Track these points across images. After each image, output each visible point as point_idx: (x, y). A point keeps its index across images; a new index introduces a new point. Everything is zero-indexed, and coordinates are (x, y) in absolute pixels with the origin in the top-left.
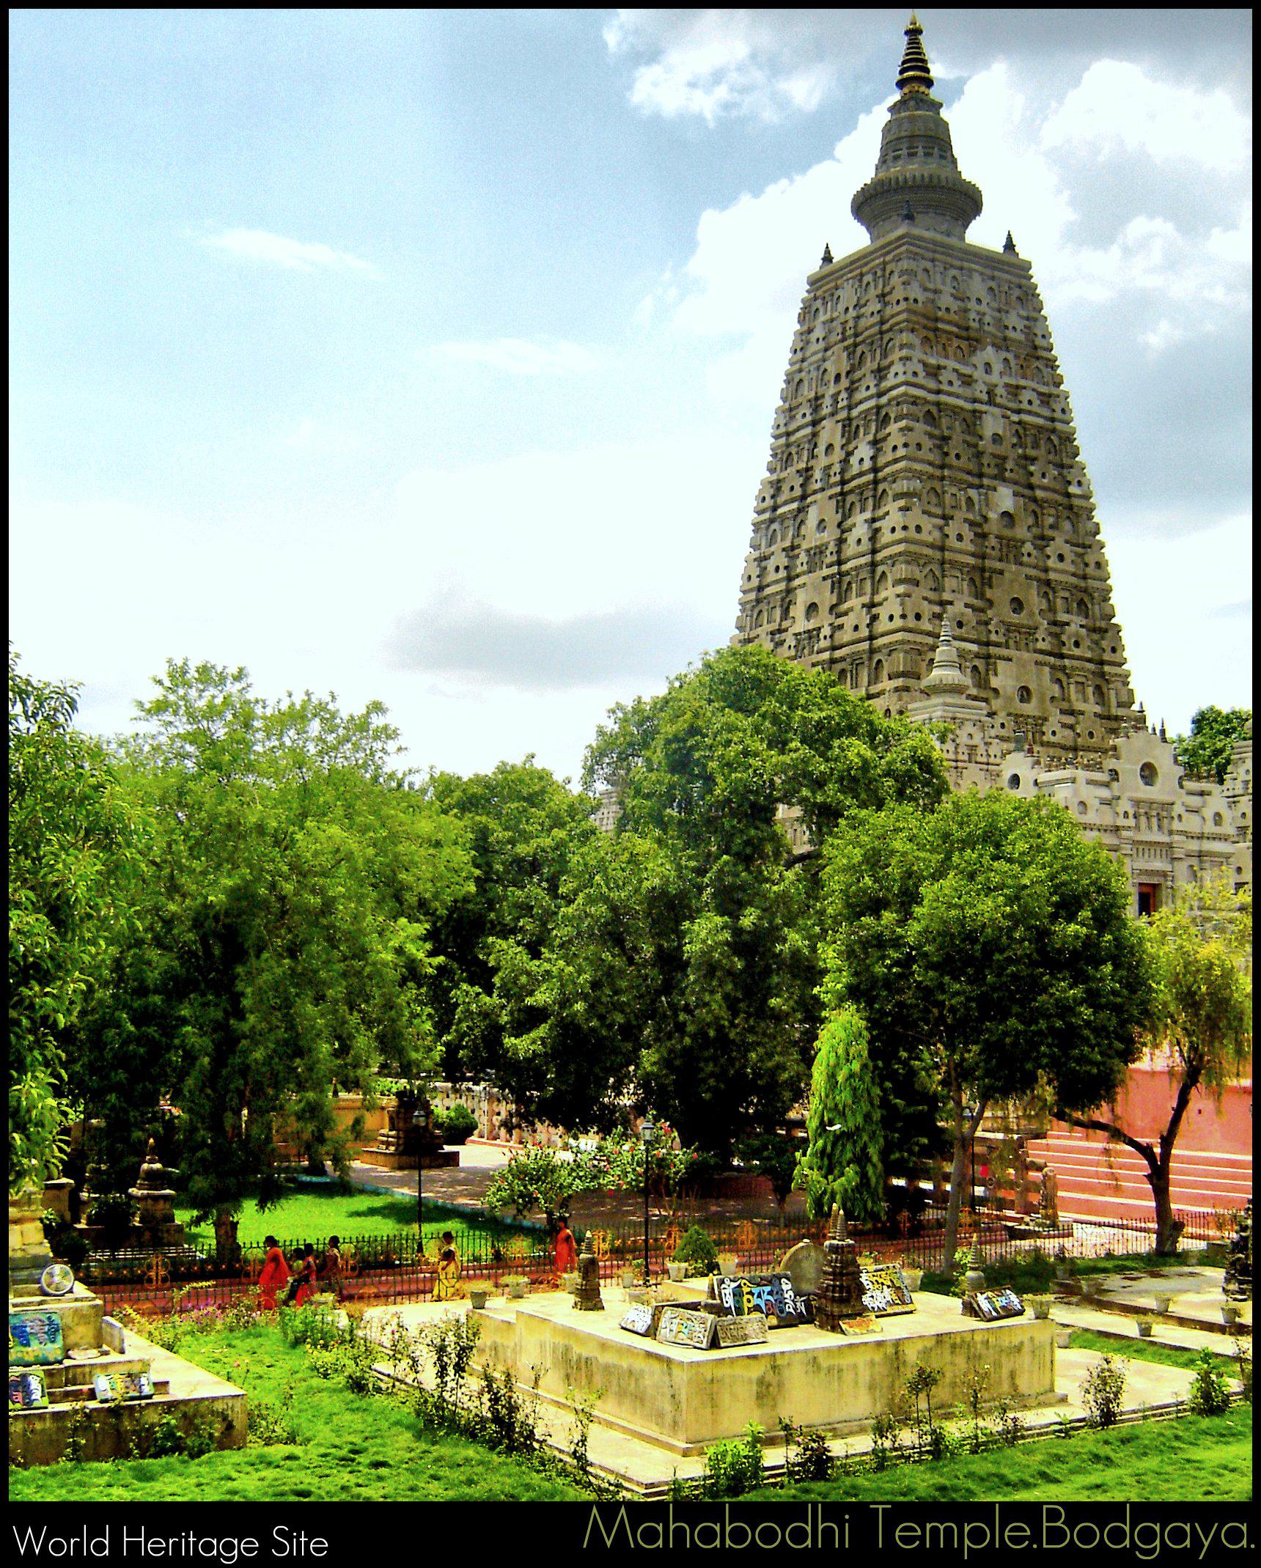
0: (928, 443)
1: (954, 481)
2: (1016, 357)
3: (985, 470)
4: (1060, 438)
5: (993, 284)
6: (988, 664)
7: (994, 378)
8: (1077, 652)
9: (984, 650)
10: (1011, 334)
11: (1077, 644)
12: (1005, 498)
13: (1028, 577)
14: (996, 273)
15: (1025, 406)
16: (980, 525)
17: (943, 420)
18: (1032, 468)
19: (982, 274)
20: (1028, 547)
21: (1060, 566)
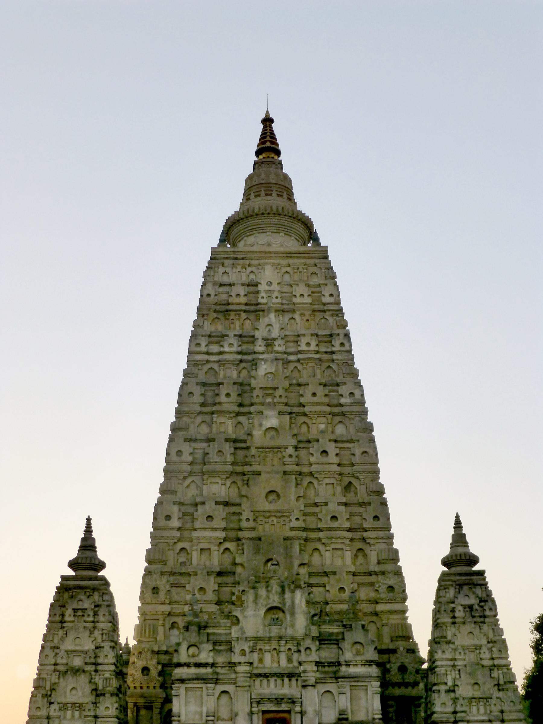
0: (197, 391)
1: (221, 413)
2: (302, 315)
3: (255, 400)
4: (338, 364)
5: (288, 269)
6: (238, 545)
7: (275, 333)
8: (335, 525)
9: (232, 534)
10: (298, 300)
11: (334, 518)
12: (272, 420)
13: (285, 473)
14: (291, 261)
15: (303, 347)
16: (245, 441)
17: (222, 372)
18: (301, 392)
19: (273, 264)
20: (291, 450)
21: (324, 459)
